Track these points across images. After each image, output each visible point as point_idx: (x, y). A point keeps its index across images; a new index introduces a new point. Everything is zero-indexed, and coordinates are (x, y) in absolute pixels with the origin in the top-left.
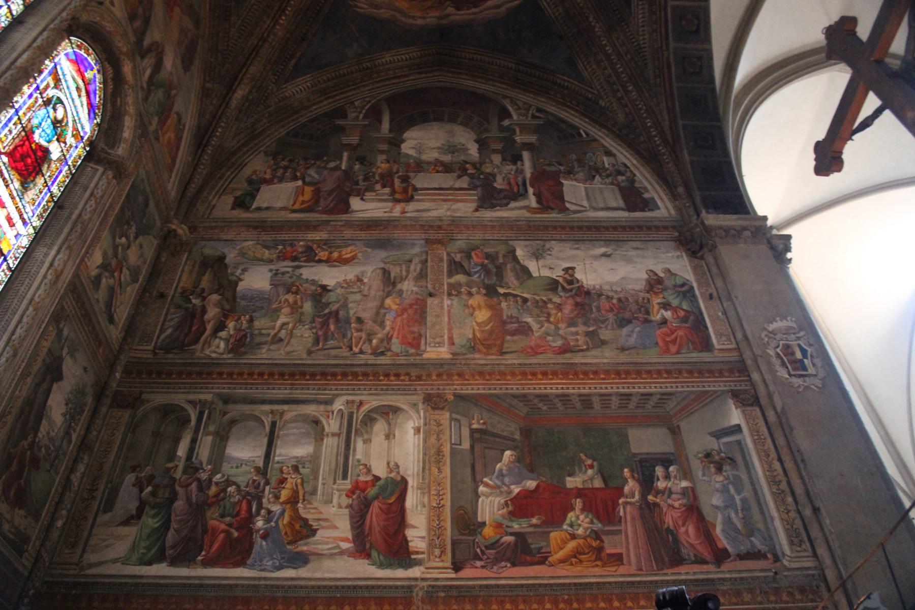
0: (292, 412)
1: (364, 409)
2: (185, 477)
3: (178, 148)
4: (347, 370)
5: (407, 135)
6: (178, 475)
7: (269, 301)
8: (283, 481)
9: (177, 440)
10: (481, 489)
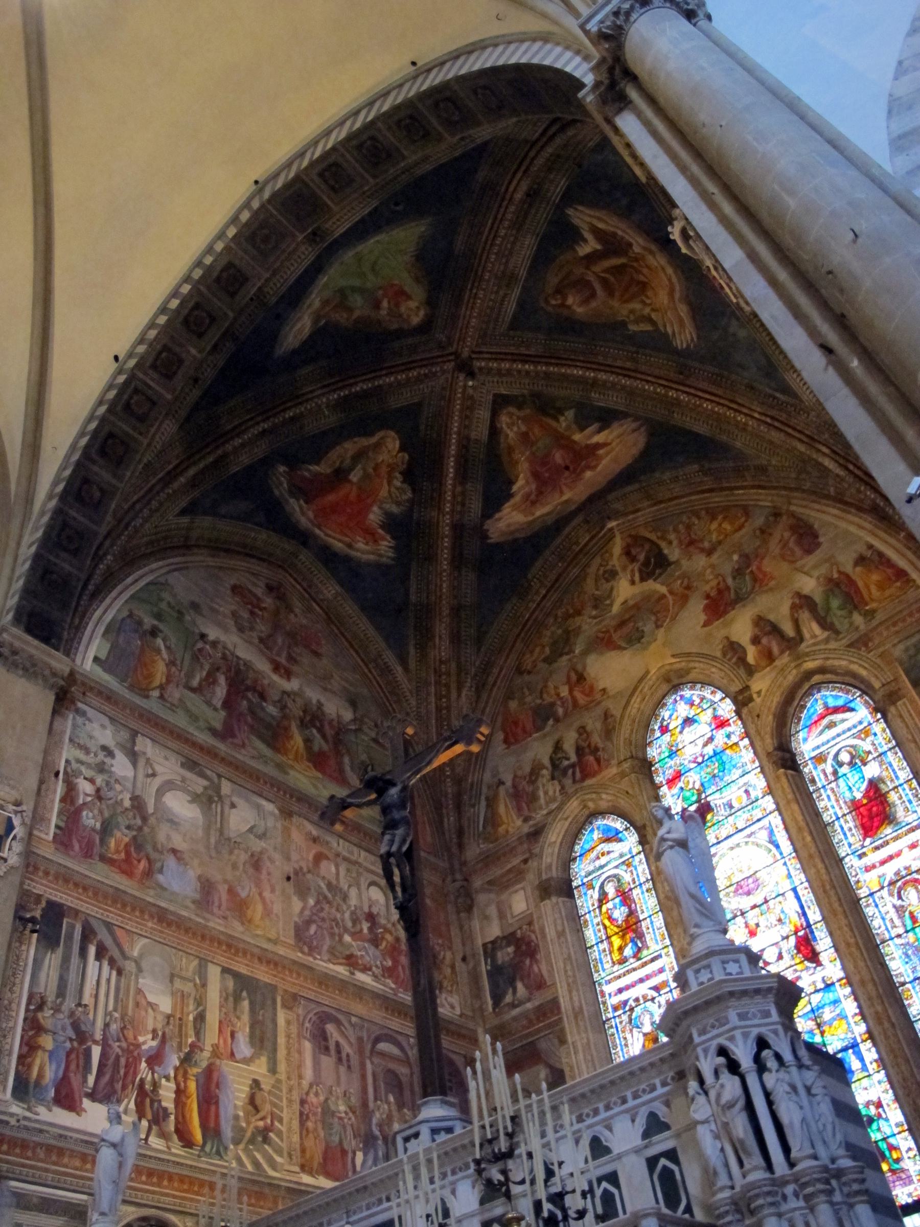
3: (889, 563)
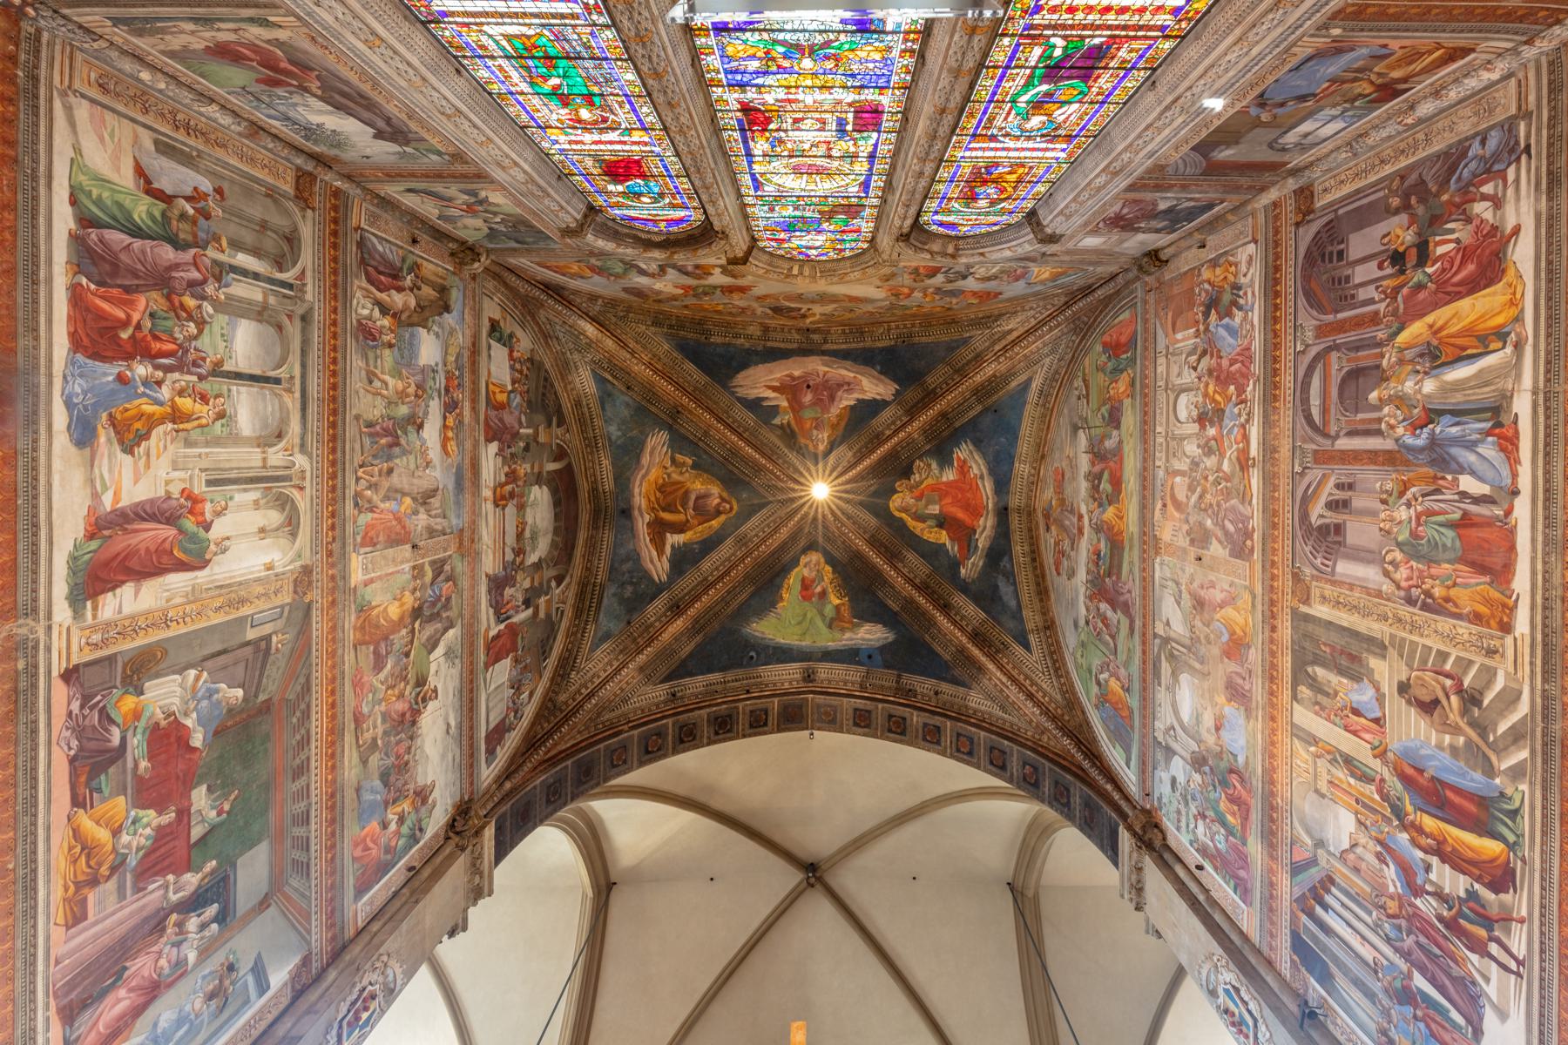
0: (292, 402)
1: (296, 494)
2: (208, 262)
4: (339, 466)
5: (545, 488)
6: (211, 253)
7: (409, 365)
8: (204, 399)
9: (256, 252)
10: (192, 673)
